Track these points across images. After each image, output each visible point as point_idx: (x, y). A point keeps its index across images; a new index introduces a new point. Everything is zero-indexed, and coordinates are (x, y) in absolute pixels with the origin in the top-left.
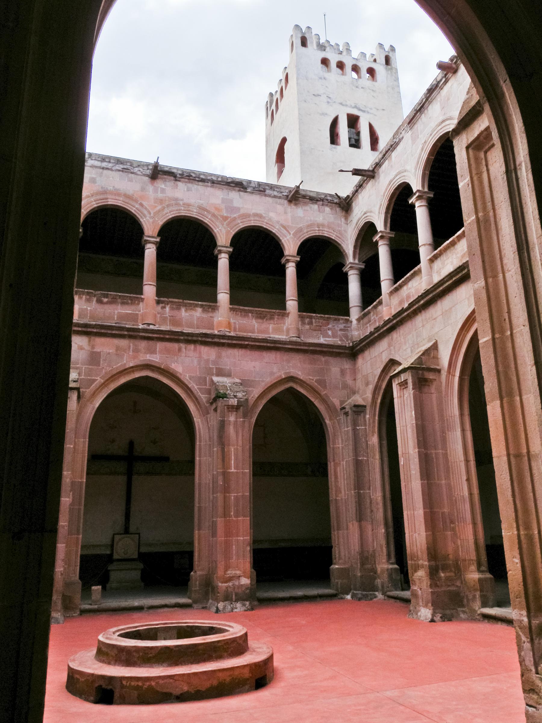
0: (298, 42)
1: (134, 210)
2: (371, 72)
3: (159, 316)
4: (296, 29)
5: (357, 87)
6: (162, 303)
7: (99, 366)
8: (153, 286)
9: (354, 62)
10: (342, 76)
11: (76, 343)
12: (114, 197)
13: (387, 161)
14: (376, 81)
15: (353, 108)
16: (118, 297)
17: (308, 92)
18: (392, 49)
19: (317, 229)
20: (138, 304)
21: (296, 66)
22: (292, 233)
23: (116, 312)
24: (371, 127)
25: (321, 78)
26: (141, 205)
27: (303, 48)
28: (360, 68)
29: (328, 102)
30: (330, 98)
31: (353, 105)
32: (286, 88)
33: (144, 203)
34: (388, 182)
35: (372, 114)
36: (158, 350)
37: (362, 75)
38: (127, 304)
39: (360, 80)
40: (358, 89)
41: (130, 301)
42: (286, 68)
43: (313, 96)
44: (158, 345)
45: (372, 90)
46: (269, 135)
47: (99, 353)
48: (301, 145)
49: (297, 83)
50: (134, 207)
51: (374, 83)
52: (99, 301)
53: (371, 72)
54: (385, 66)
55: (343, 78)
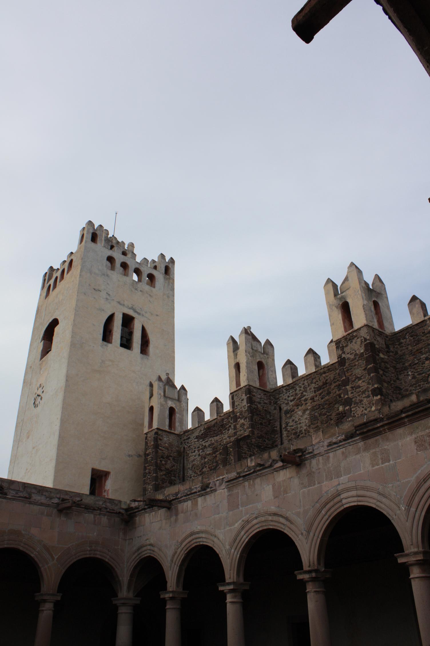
0: (88, 237)
2: (151, 277)
4: (89, 225)
5: (136, 289)
9: (137, 266)
10: (124, 276)
13: (189, 503)
14: (154, 287)
15: (130, 308)
17: (90, 285)
18: (172, 261)
19: (89, 549)
21: (82, 259)
22: (56, 557)
24: (144, 329)
25: (104, 275)
27: (93, 244)
28: (141, 273)
29: (107, 299)
30: (109, 295)
31: (130, 306)
32: (68, 273)
34: (188, 532)
35: (146, 318)
37: (143, 279)
39: (141, 283)
40: (137, 291)
42: (72, 253)
43: (94, 290)
45: (150, 295)
46: (41, 306)
48: (72, 337)
49: (80, 275)
51: (152, 288)
53: (151, 277)
54: (164, 275)
55: (125, 278)
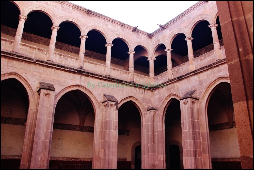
1: (205, 18)
3: (222, 54)
6: (222, 49)
7: (202, 85)
8: (218, 43)
11: (194, 79)
12: (196, 19)
16: (206, 55)
20: (214, 53)
23: (207, 61)
26: (206, 15)
33: (206, 14)
36: (222, 70)
38: (210, 55)
41: (210, 54)
44: (222, 67)
47: (202, 80)
50: (204, 17)
52: (201, 60)
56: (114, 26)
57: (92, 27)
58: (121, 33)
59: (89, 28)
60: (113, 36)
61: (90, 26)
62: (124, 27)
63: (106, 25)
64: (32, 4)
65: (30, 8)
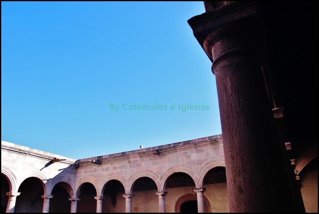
56: (201, 151)
57: (168, 172)
58: (214, 157)
59: (164, 177)
60: (202, 171)
61: (165, 173)
62: (219, 144)
63: (188, 156)
64: (103, 177)
65: (103, 183)
